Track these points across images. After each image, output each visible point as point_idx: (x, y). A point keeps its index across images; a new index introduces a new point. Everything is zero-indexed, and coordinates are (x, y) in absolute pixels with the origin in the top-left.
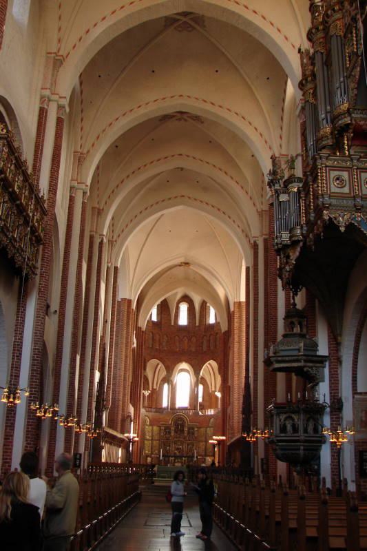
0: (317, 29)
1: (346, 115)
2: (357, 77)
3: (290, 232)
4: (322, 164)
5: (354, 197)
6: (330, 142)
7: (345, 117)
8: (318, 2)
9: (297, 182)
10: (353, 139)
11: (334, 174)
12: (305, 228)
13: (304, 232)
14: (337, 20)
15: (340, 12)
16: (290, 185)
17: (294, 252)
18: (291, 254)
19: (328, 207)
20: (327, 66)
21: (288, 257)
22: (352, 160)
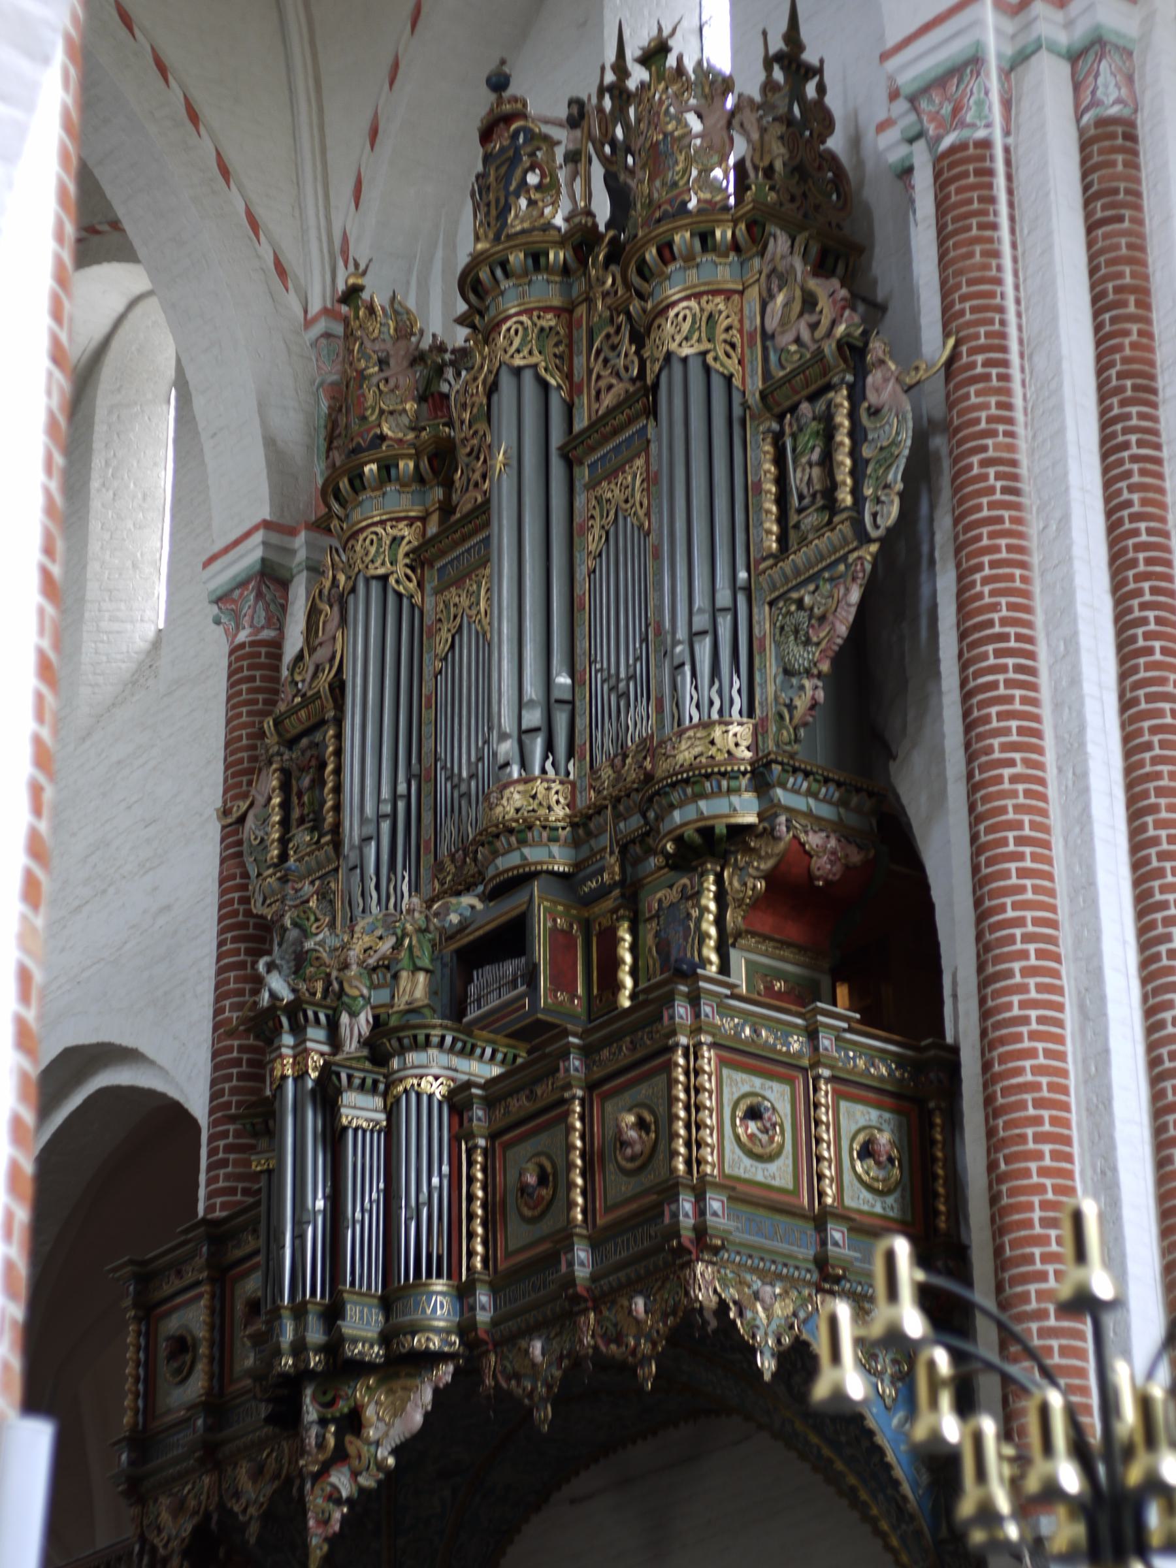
0: (537, 258)
1: (744, 782)
2: (843, 630)
3: (387, 1303)
4: (696, 1030)
5: (820, 1219)
6: (559, 859)
7: (737, 791)
8: (547, 122)
9: (451, 1050)
10: (758, 903)
11: (740, 1084)
12: (483, 1298)
13: (483, 1317)
14: (715, 293)
15: (732, 256)
16: (413, 1057)
17: (398, 1411)
18: (370, 1412)
19: (716, 1250)
20: (570, 464)
21: (353, 1422)
22: (812, 1035)
